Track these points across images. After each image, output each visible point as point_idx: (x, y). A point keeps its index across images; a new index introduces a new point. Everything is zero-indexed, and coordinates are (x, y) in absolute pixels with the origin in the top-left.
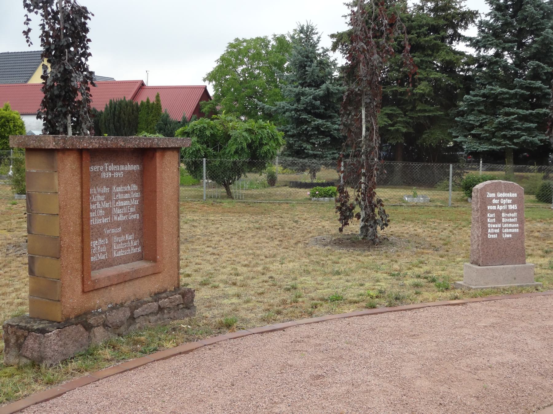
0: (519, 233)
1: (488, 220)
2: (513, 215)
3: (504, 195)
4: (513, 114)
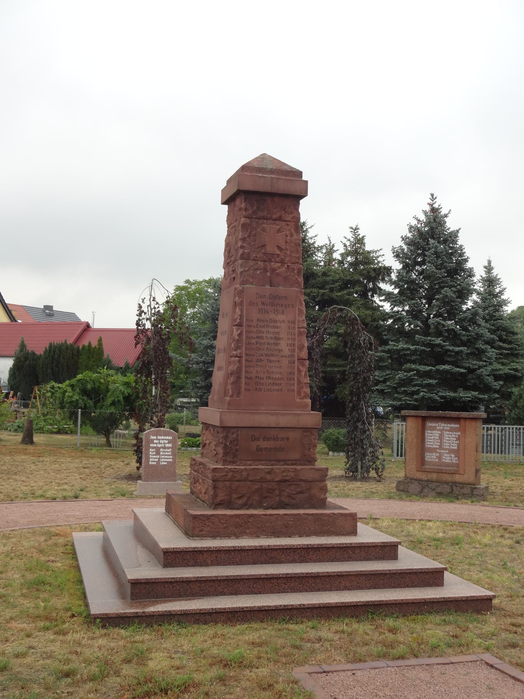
0: (172, 462)
1: (150, 453)
2: (168, 450)
3: (163, 437)
4: (413, 370)
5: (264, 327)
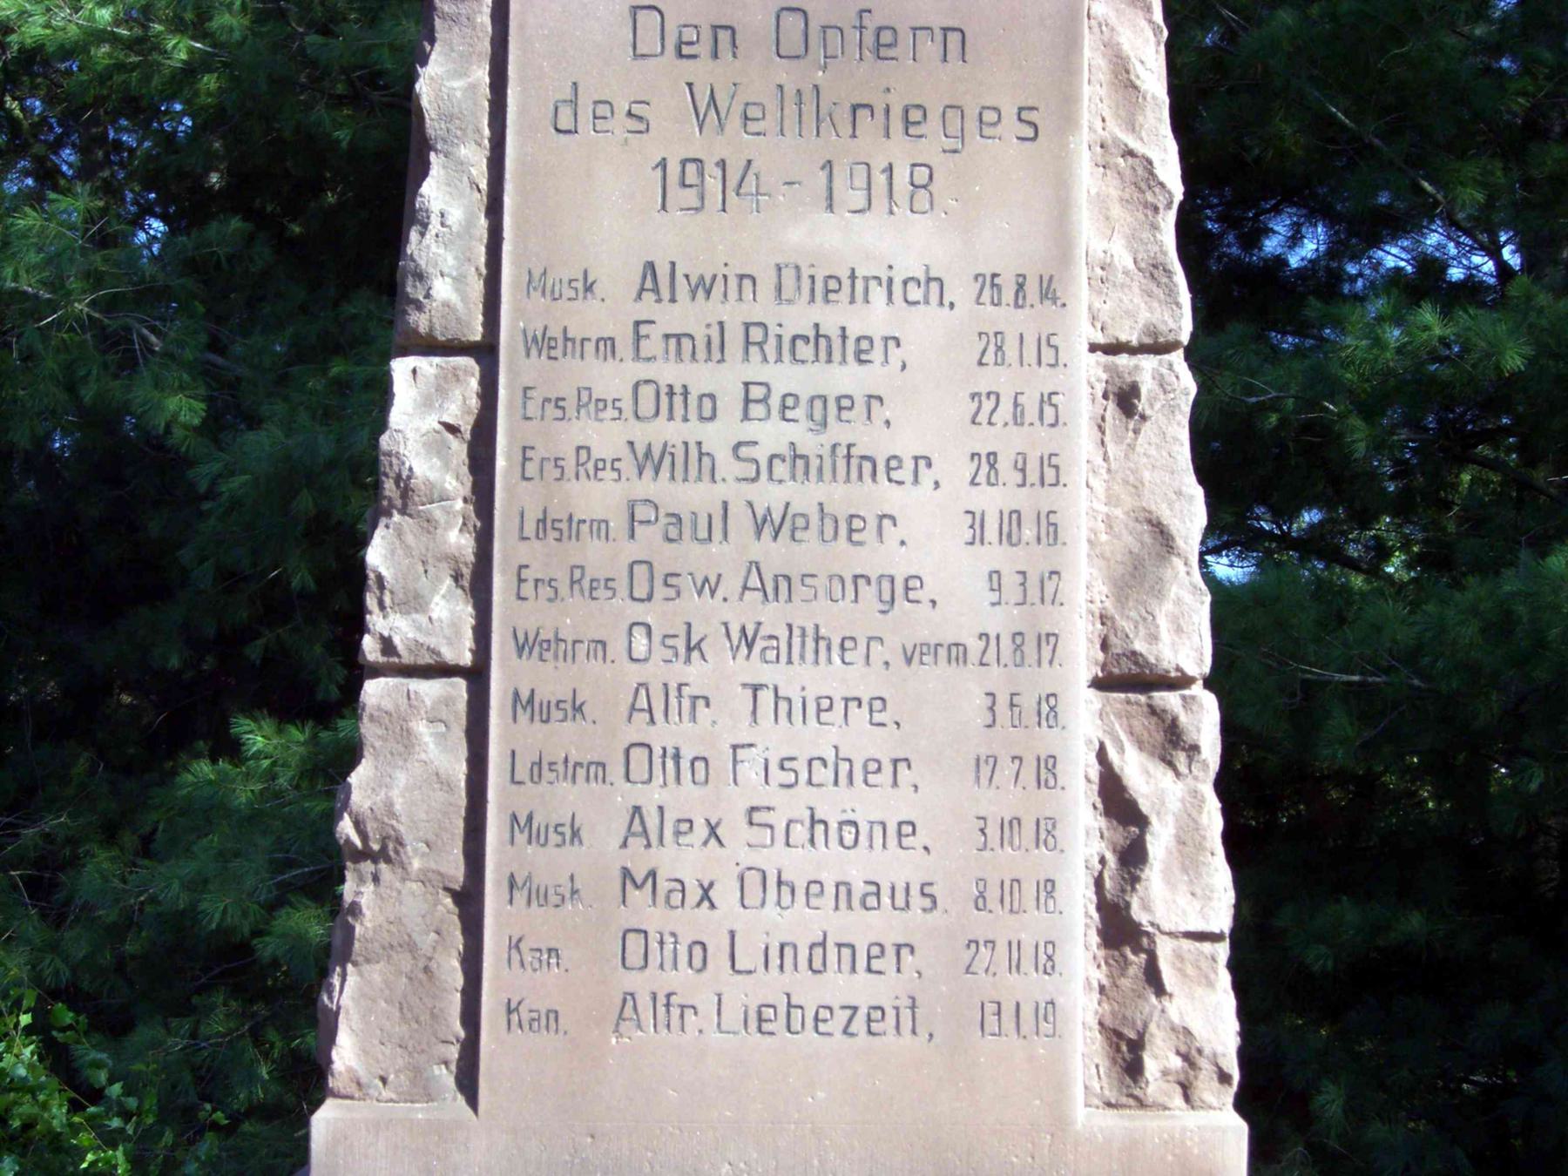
5: (716, 348)
